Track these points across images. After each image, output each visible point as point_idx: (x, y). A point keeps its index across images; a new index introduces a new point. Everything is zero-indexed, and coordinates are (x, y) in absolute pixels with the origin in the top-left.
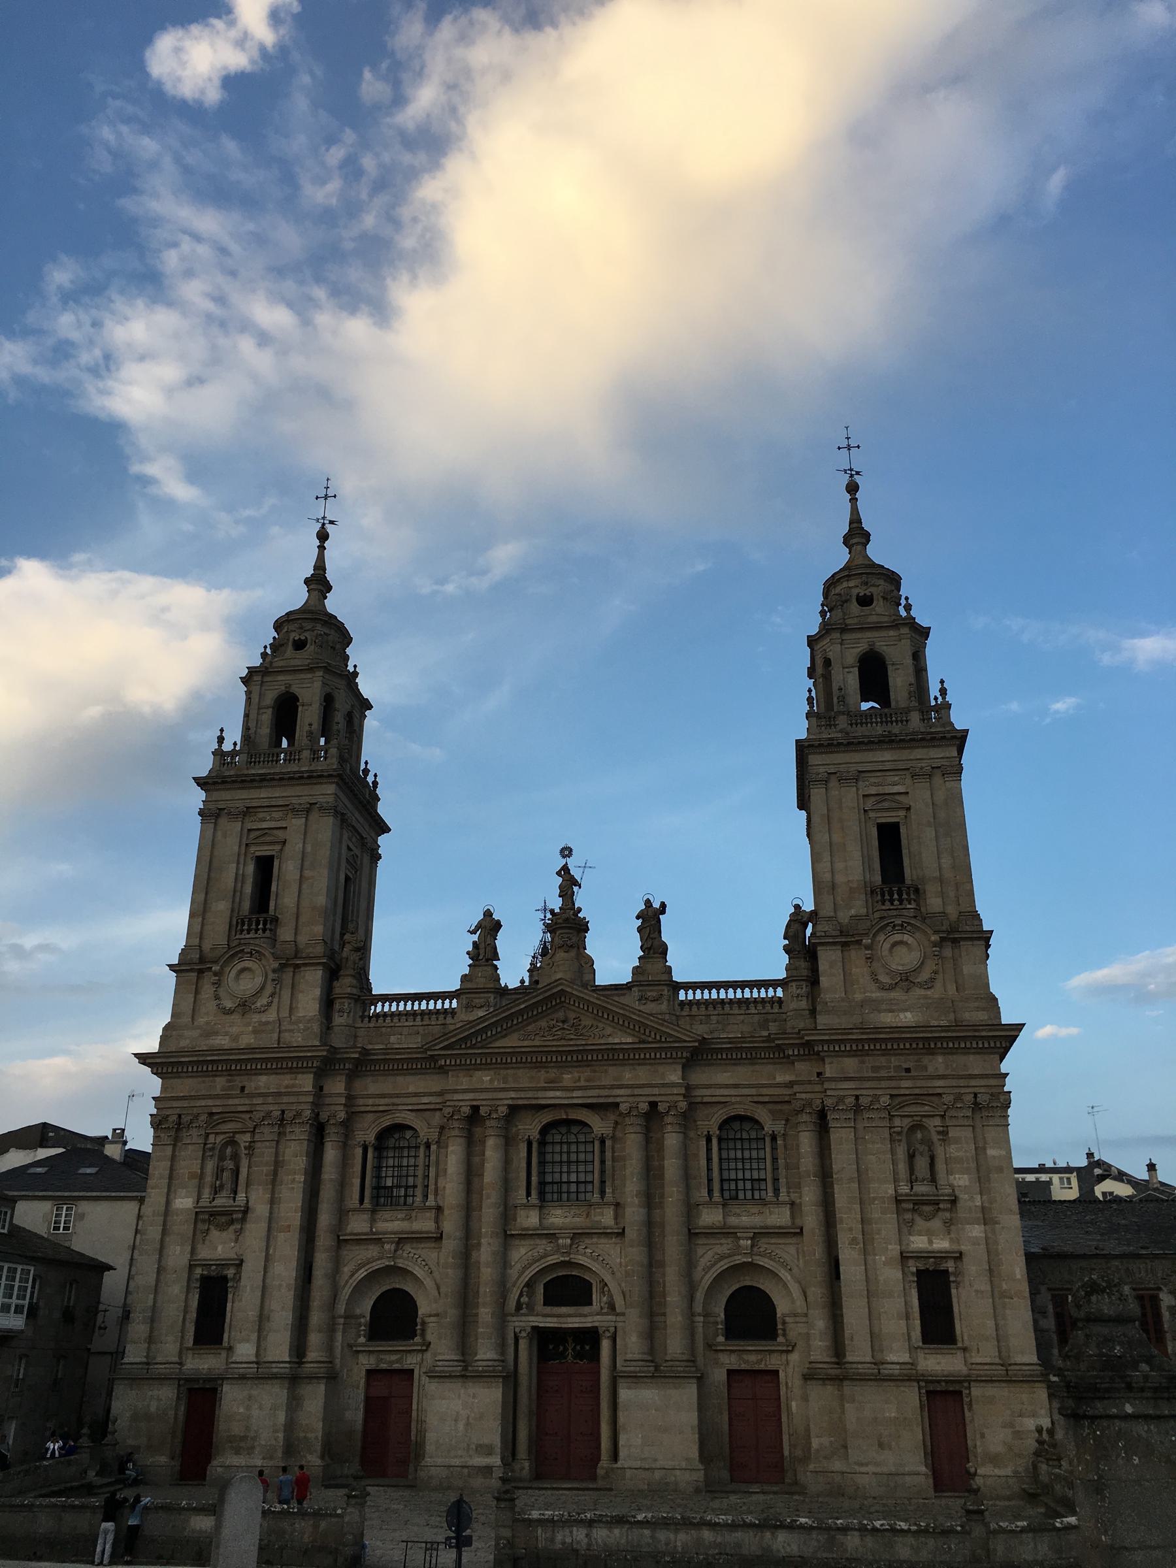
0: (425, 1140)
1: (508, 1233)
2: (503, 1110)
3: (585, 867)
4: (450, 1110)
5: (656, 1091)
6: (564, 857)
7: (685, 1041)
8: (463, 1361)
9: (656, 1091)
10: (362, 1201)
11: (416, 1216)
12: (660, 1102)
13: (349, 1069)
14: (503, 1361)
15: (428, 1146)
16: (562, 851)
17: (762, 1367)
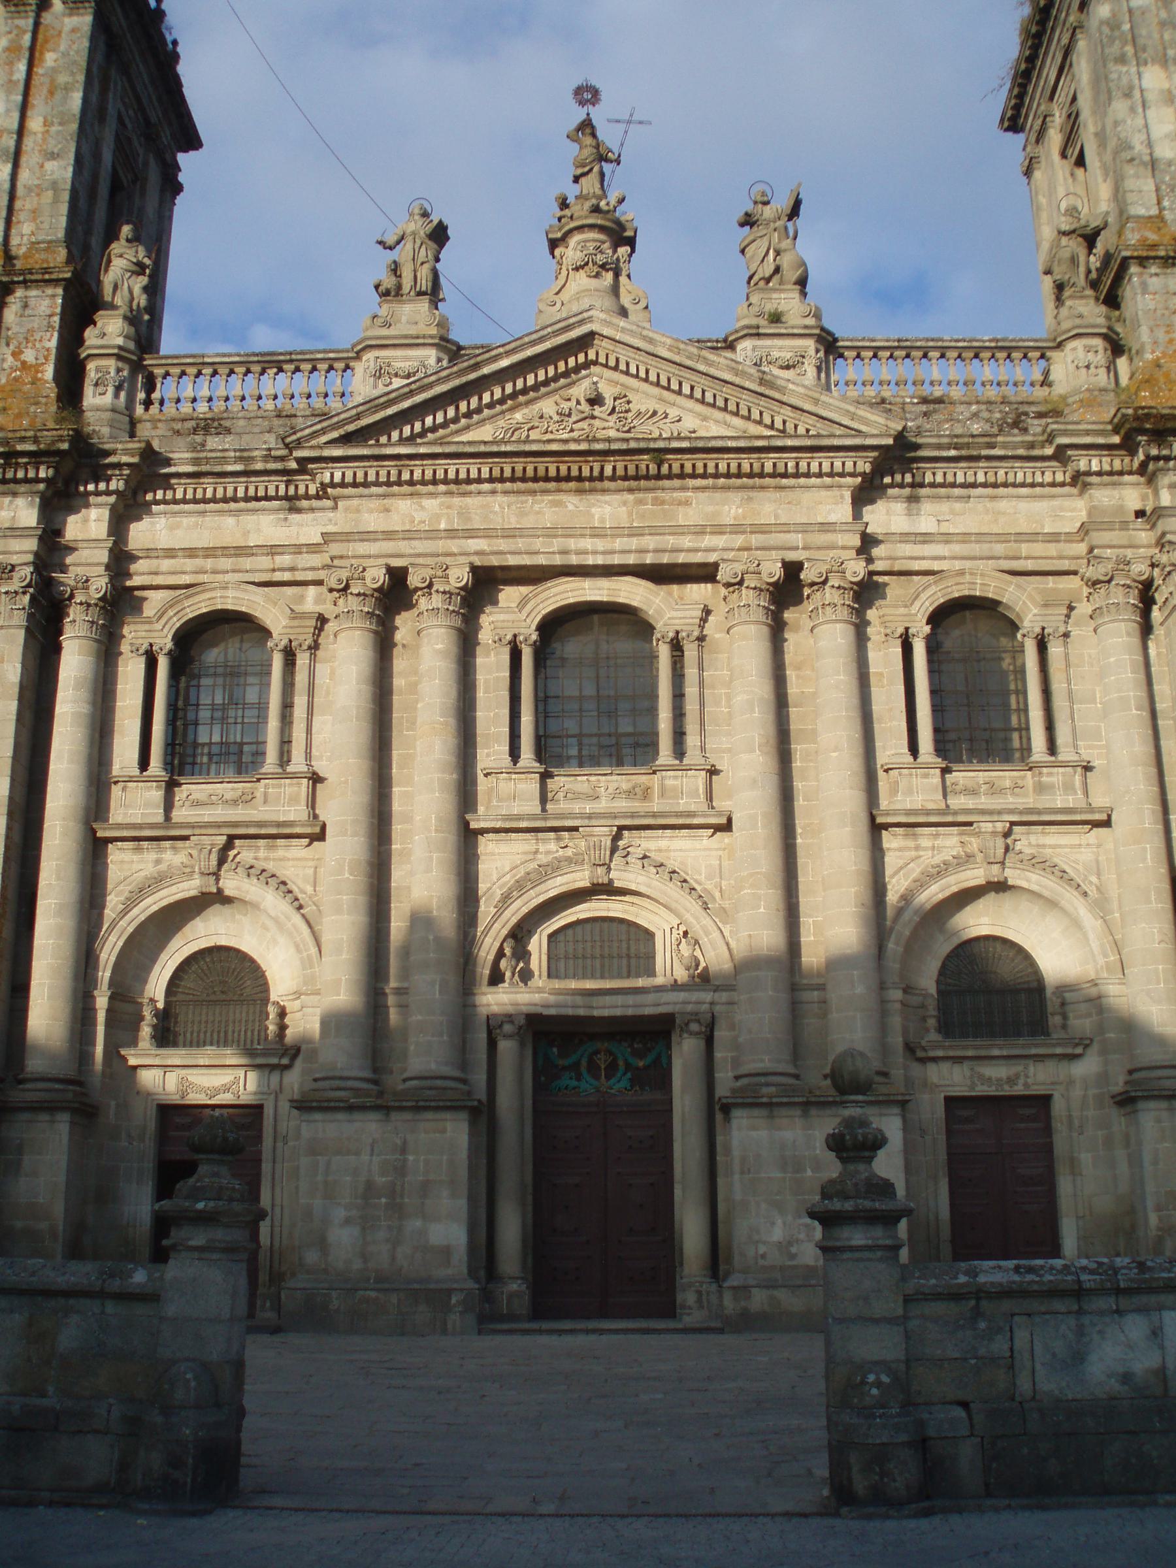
0: (284, 642)
1: (473, 825)
2: (460, 576)
3: (629, 122)
4: (344, 575)
5: (798, 539)
6: (582, 103)
7: (866, 435)
8: (376, 1082)
9: (798, 539)
10: (144, 763)
11: (265, 794)
12: (808, 560)
13: (117, 492)
14: (464, 1081)
15: (290, 656)
16: (578, 91)
17: (1019, 1090)
